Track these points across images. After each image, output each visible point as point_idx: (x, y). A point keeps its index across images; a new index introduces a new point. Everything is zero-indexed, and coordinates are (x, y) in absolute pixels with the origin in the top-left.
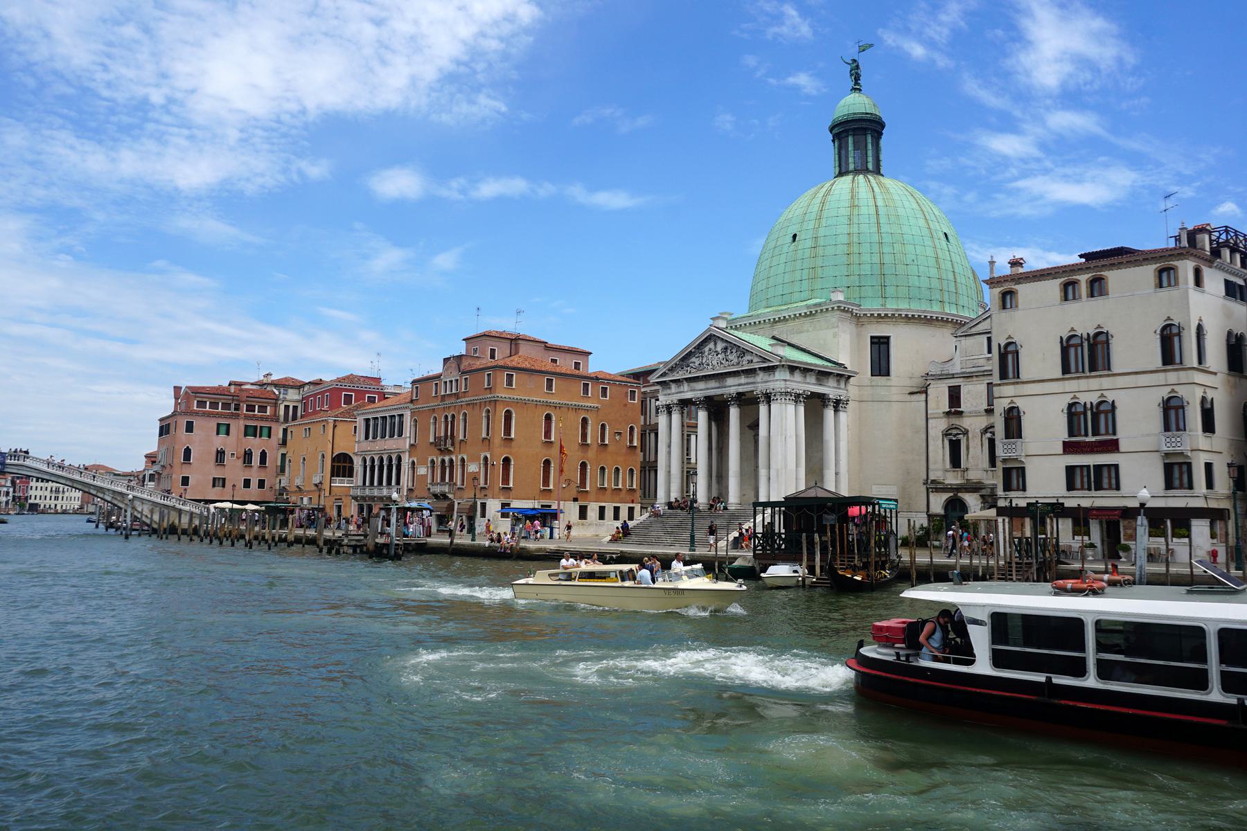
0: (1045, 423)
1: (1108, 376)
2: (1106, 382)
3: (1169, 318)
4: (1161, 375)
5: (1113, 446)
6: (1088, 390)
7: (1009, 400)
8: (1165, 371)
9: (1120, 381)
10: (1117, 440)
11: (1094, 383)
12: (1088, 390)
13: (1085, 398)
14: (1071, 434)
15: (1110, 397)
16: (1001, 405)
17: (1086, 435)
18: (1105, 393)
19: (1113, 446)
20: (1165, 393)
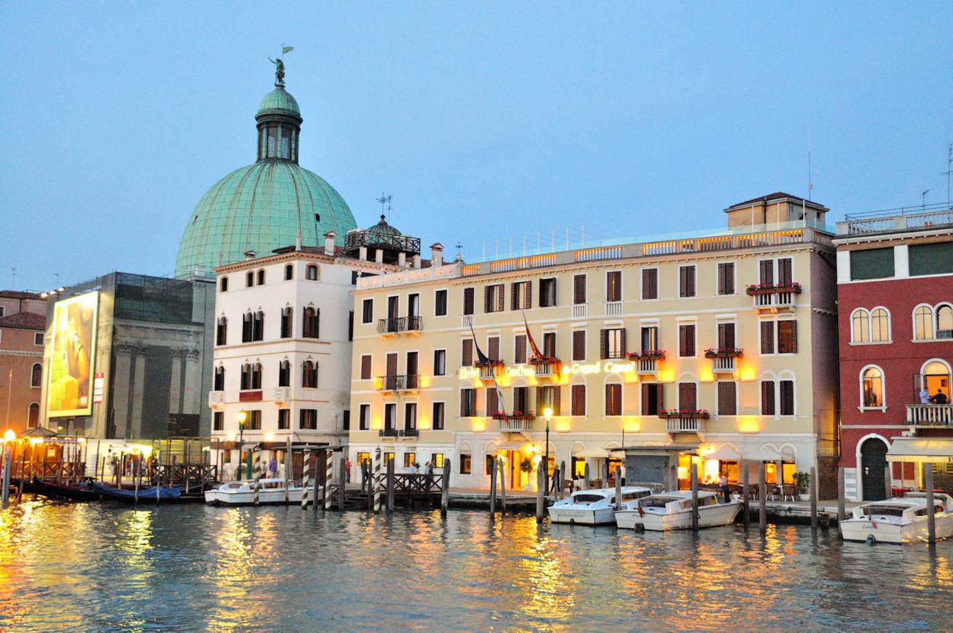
4: (282, 344)
5: (258, 397)
6: (253, 353)
8: (284, 342)
10: (260, 393)
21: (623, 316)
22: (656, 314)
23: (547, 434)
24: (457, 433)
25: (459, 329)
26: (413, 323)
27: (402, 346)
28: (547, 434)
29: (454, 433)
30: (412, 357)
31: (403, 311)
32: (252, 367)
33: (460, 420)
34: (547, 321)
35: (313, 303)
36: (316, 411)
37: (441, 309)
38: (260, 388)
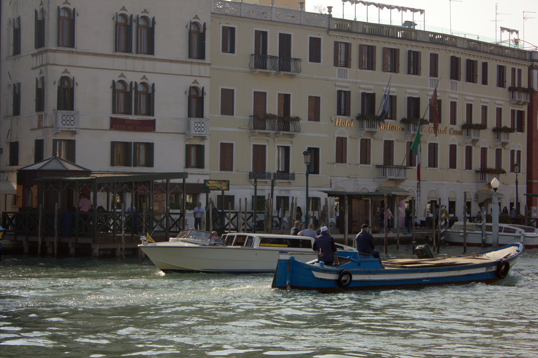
0: (94, 100)
1: (150, 59)
2: (148, 65)
3: (196, 17)
4: (188, 66)
5: (150, 126)
6: (134, 70)
7: (62, 69)
9: (160, 66)
10: (154, 122)
11: (139, 64)
12: (134, 70)
13: (132, 78)
14: (114, 112)
15: (151, 79)
16: (54, 75)
17: (129, 112)
18: (147, 75)
19: (150, 126)
20: (189, 82)
21: (458, 92)
22: (471, 94)
23: (517, 185)
24: (332, 178)
25: (335, 78)
26: (285, 62)
27: (273, 86)
28: (517, 185)
29: (329, 178)
30: (285, 100)
31: (273, 48)
32: (134, 86)
33: (335, 166)
34: (411, 86)
35: (126, 8)
36: (153, 144)
37: (315, 55)
38: (153, 115)
